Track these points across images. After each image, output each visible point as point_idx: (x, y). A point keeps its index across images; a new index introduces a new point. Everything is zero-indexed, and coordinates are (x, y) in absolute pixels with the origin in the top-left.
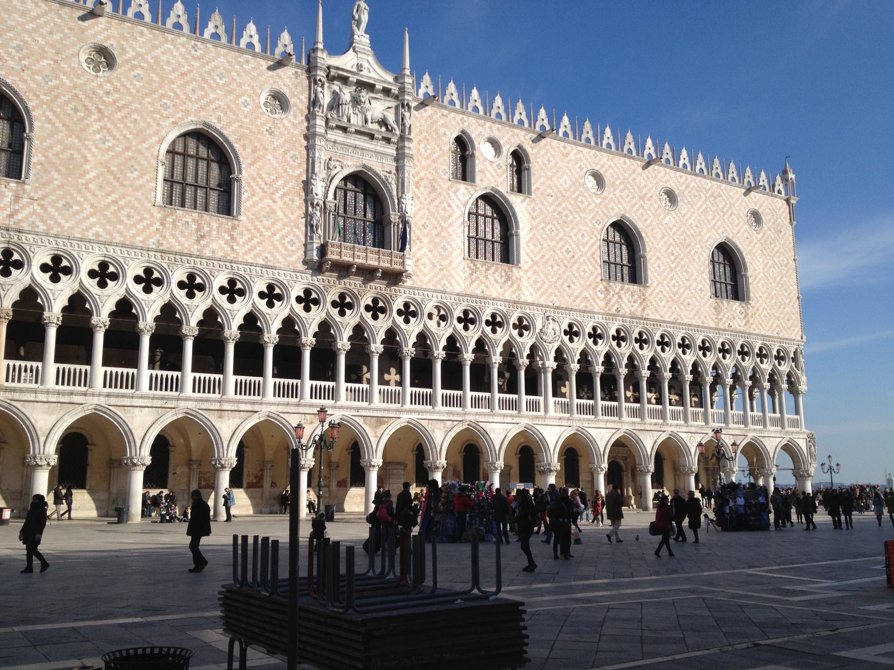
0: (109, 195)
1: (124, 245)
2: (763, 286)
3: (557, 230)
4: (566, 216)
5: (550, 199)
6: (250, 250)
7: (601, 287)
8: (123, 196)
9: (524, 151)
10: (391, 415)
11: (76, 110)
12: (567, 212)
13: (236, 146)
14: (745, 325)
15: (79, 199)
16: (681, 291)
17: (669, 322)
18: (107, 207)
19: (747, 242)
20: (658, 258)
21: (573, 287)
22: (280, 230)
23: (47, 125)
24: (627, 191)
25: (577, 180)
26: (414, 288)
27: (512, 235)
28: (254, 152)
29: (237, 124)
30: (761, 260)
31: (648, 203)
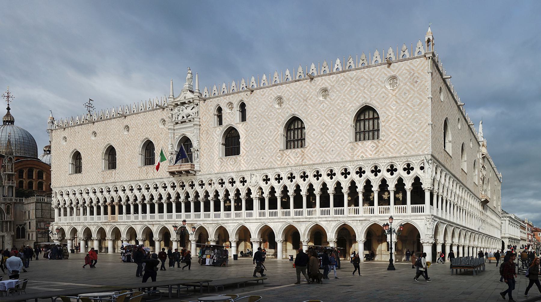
1: (132, 181)
2: (394, 125)
3: (258, 133)
4: (263, 125)
5: (255, 120)
7: (279, 154)
12: (263, 123)
14: (376, 153)
16: (328, 145)
17: (317, 164)
19: (384, 99)
20: (314, 130)
21: (265, 158)
24: (297, 100)
25: (269, 105)
30: (394, 108)
31: (309, 101)
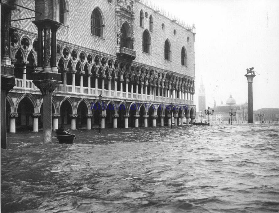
0: (83, 31)
6: (107, 49)
7: (164, 62)
8: (85, 32)
9: (152, 17)
10: (131, 102)
11: (76, 2)
13: (104, 15)
15: (78, 33)
18: (83, 35)
22: (112, 43)
23: (71, 7)
26: (135, 62)
27: (149, 44)
28: (107, 16)
29: (104, 7)
